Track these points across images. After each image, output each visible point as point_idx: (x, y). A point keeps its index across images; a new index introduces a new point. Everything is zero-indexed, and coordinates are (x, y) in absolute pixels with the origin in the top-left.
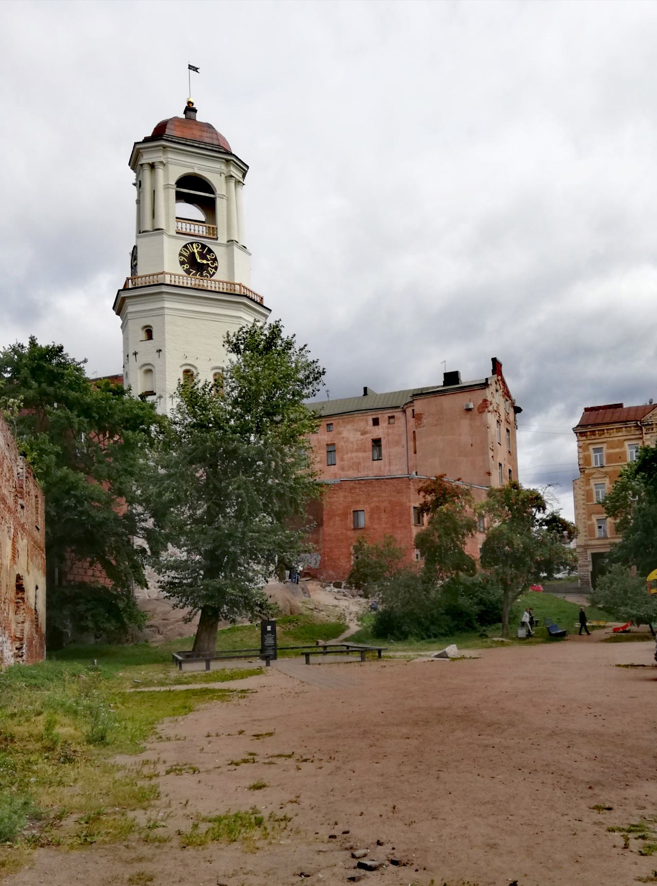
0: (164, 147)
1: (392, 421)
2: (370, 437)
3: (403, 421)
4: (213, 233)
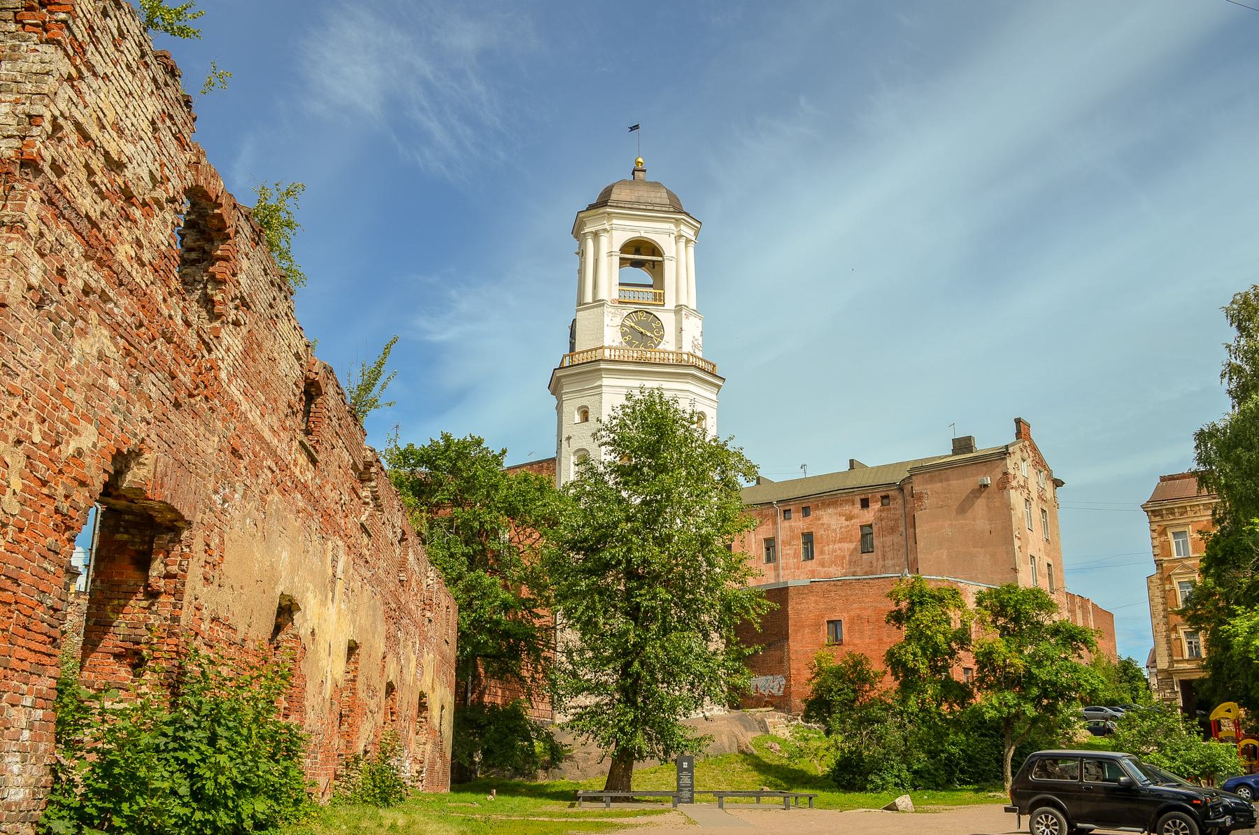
0: (609, 214)
1: (885, 501)
2: (857, 522)
3: (900, 502)
4: (660, 299)
